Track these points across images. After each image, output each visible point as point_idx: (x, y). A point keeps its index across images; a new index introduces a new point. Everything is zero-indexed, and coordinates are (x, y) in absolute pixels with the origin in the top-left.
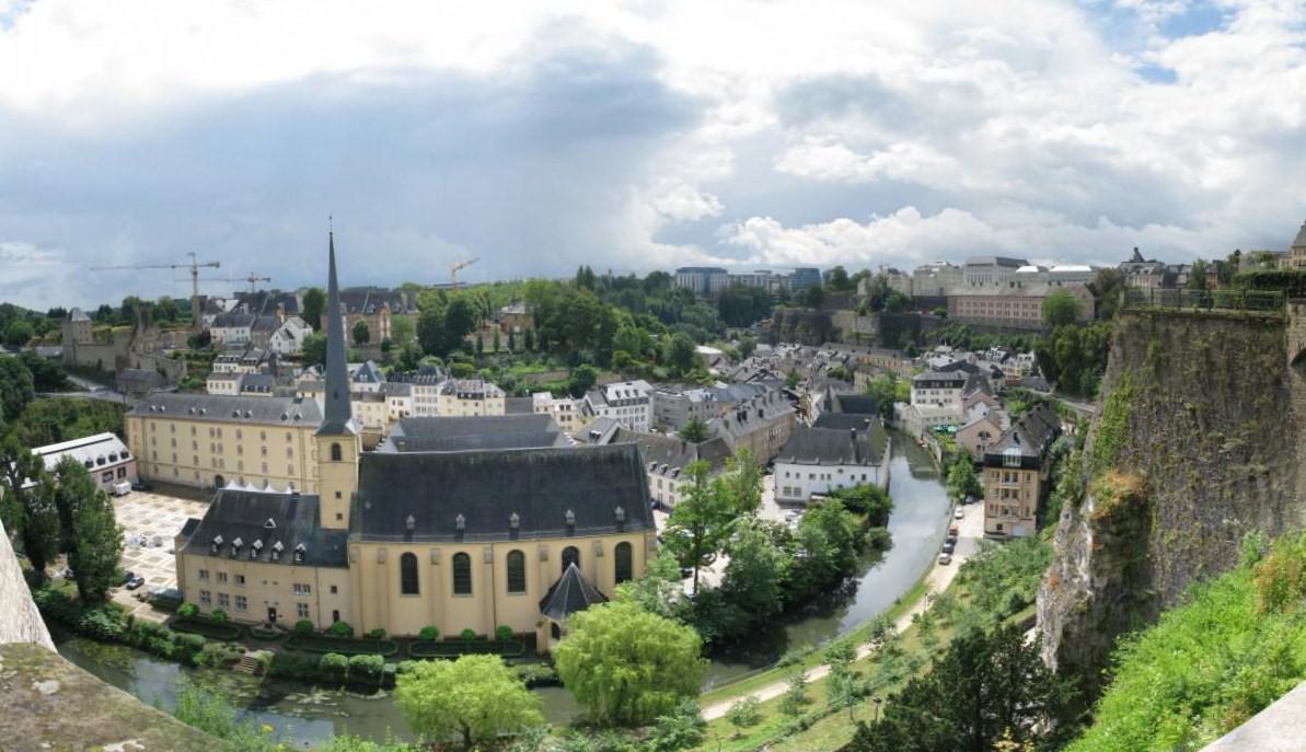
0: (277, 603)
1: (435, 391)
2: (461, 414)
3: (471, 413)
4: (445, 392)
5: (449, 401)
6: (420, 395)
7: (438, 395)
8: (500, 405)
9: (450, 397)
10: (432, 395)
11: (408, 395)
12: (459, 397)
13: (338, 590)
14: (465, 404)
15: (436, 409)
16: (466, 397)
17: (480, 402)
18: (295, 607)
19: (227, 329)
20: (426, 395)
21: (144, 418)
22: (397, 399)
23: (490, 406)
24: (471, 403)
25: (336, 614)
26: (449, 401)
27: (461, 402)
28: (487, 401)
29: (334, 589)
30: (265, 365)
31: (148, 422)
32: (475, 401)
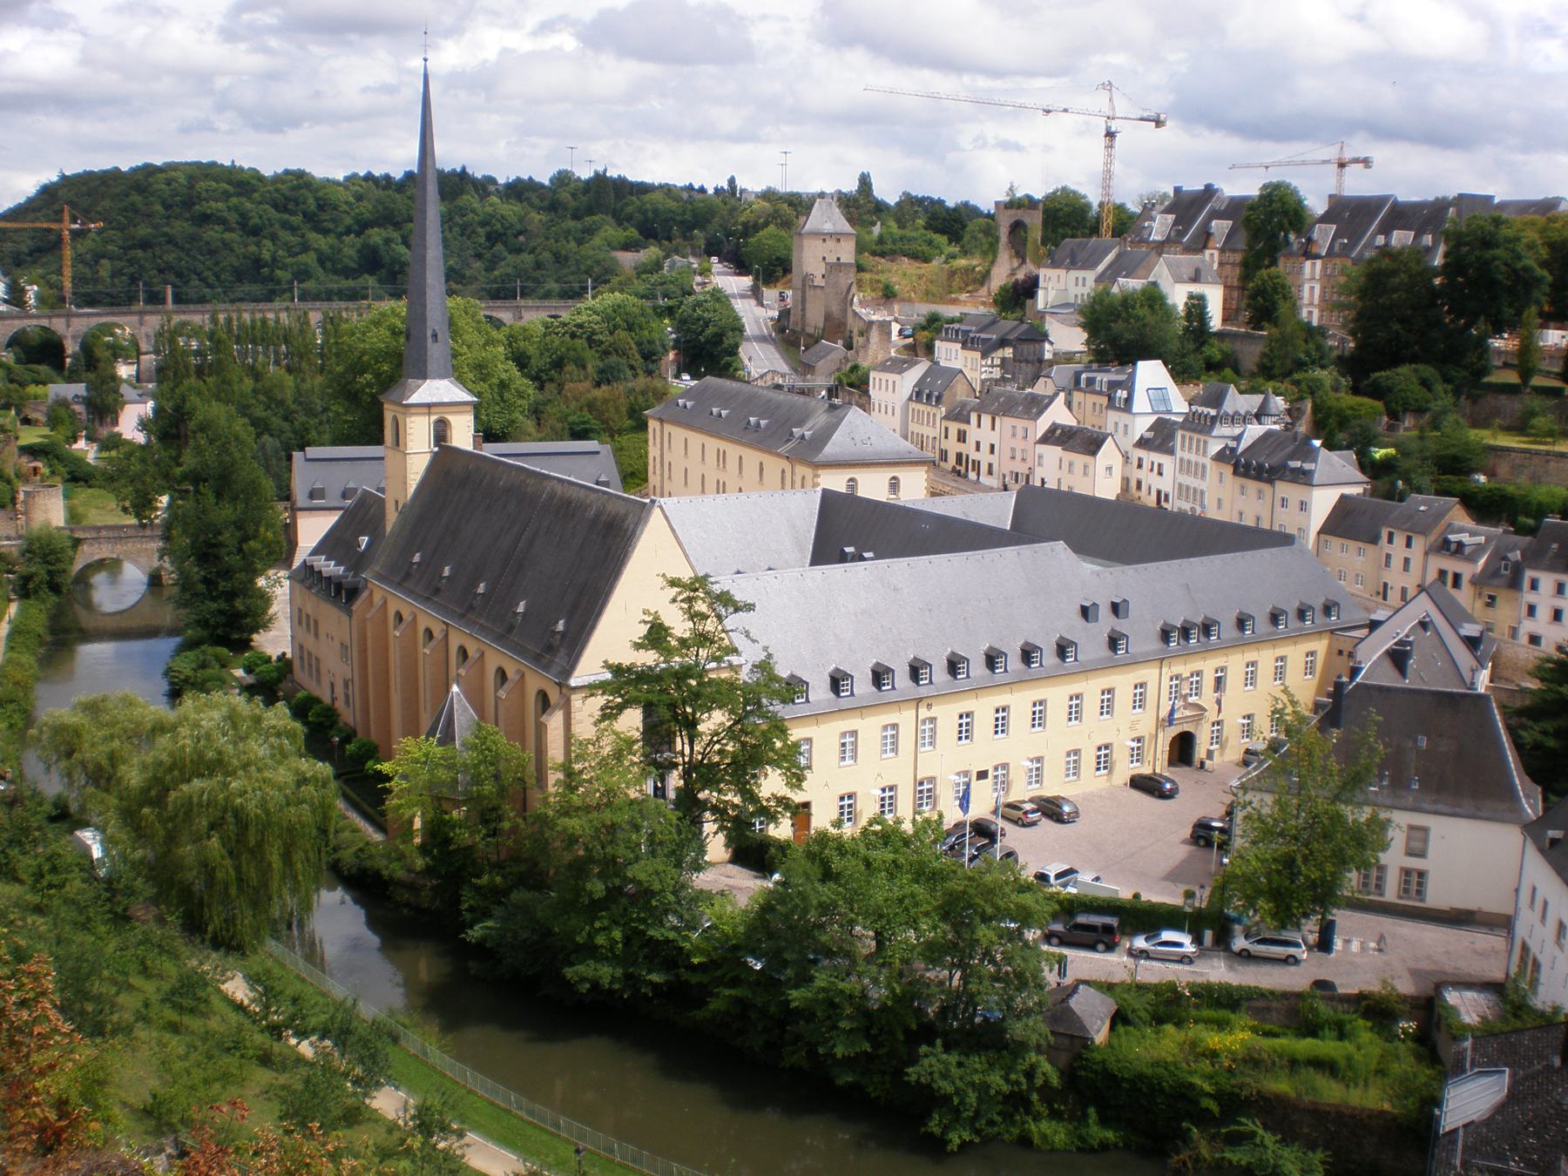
2: (1235, 520)
3: (1249, 521)
4: (1220, 457)
6: (1186, 455)
7: (1208, 462)
10: (1201, 460)
11: (1171, 452)
15: (1202, 493)
16: (1246, 475)
19: (1062, 272)
20: (1193, 457)
21: (661, 421)
22: (1157, 458)
27: (1240, 480)
30: (1008, 352)
31: (668, 428)
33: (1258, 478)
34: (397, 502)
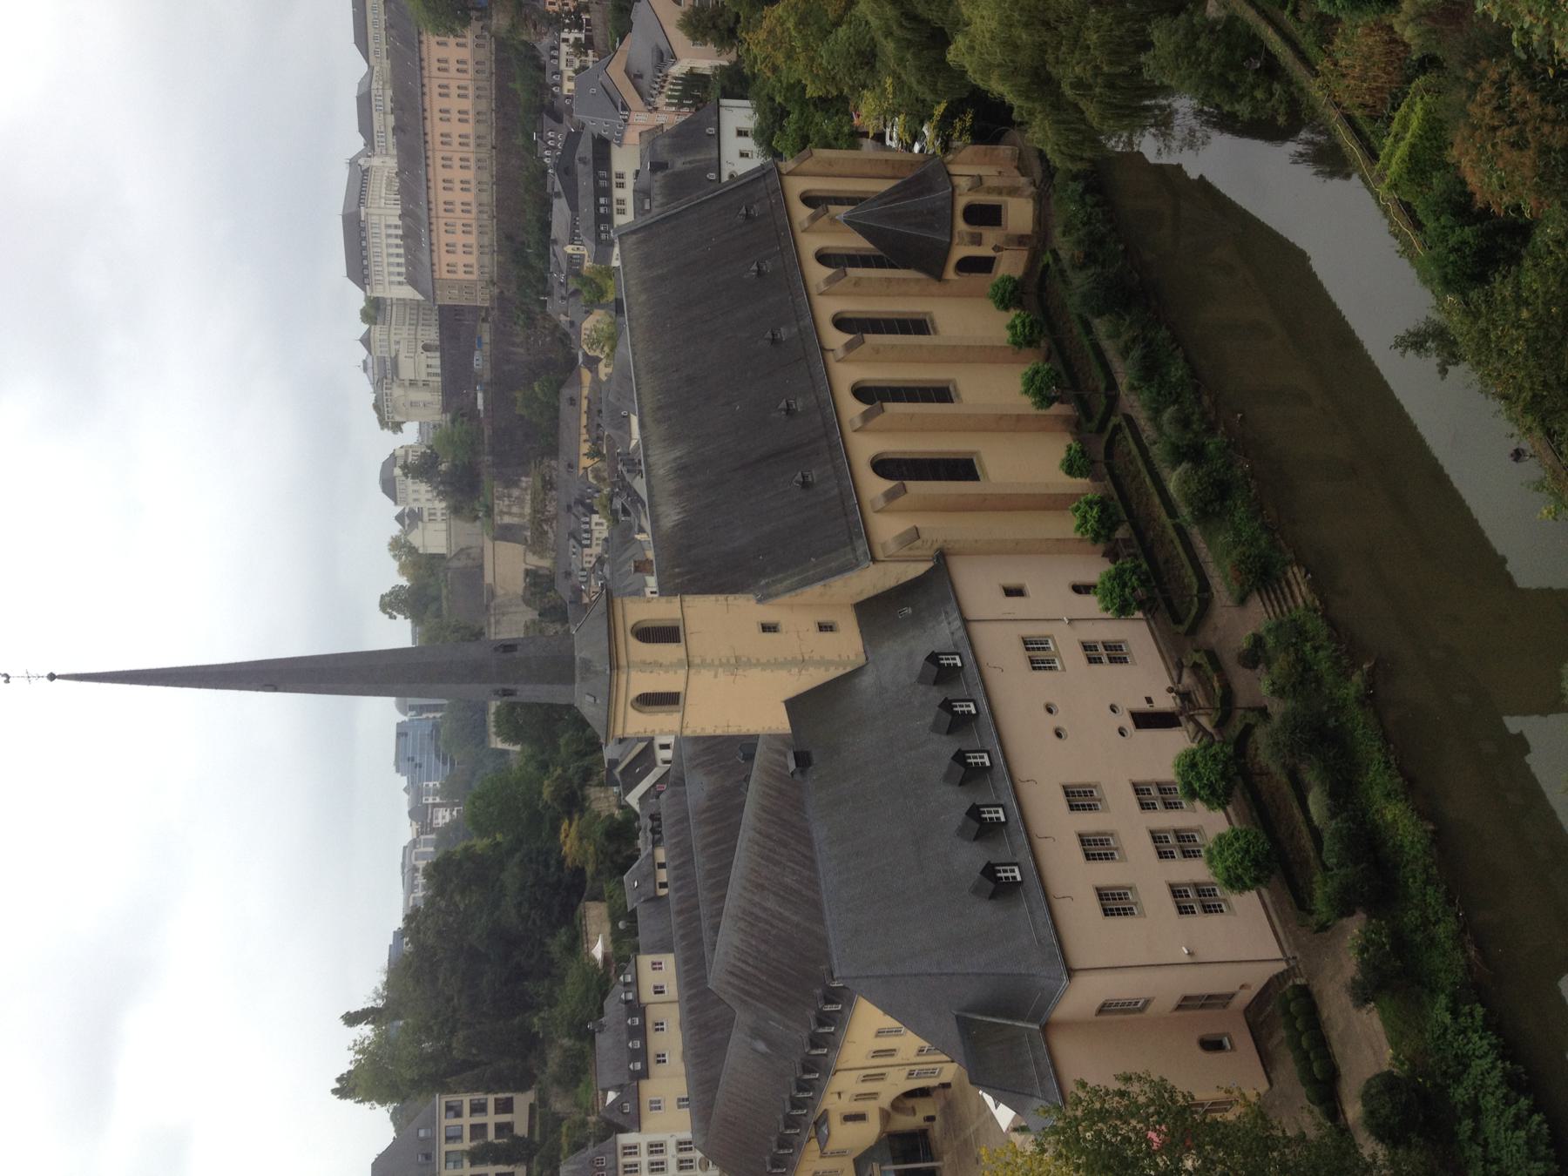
0: (1113, 709)
1: (632, 1150)
5: (656, 1106)
8: (656, 966)
9: (645, 1106)
10: (644, 1159)
12: (644, 1074)
13: (1013, 581)
14: (661, 1059)
15: (682, 1146)
16: (641, 1054)
17: (653, 1014)
18: (1106, 670)
23: (659, 990)
24: (656, 1042)
25: (1079, 589)
26: (656, 1106)
27: (654, 1068)
28: (647, 995)
29: (1014, 592)
32: (650, 1025)
33: (640, 1032)
34: (768, 628)
